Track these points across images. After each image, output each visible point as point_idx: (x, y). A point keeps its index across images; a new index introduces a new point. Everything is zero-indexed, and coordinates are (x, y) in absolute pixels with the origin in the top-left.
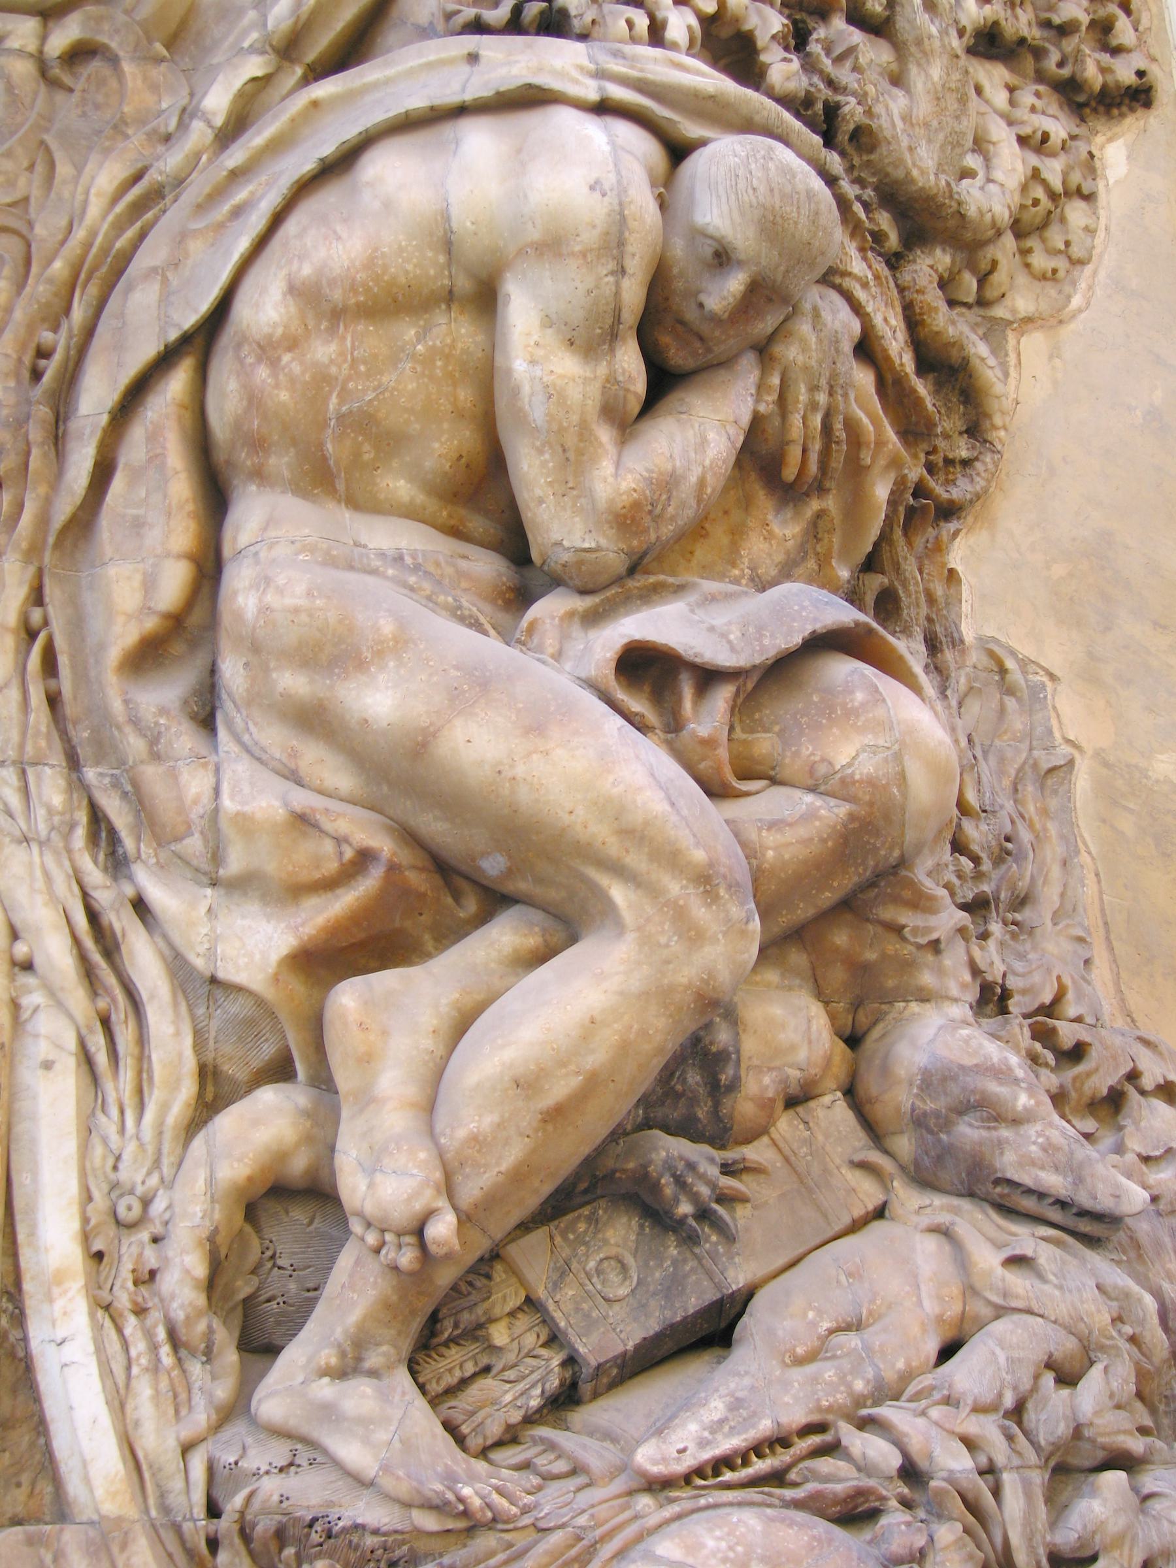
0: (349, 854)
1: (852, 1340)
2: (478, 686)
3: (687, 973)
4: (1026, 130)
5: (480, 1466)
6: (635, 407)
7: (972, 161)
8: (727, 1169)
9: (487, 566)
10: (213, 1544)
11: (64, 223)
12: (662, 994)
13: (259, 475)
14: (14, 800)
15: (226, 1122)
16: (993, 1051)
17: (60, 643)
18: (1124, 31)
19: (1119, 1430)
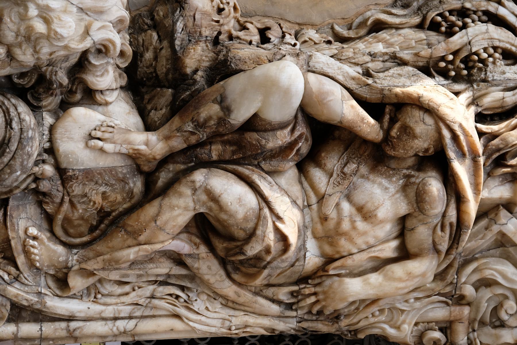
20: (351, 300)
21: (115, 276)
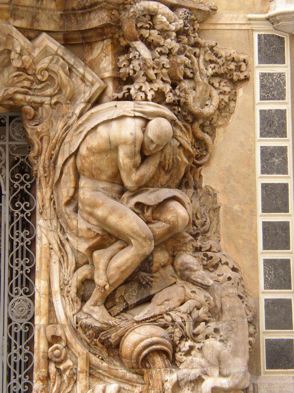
0: (95, 234)
1: (167, 302)
2: (113, 210)
3: (141, 252)
4: (221, 91)
5: (114, 318)
6: (138, 165)
7: (207, 103)
8: (152, 277)
9: (117, 188)
10: (77, 328)
11: (54, 133)
13: (84, 175)
14: (50, 225)
15: (79, 270)
17: (56, 201)
18: (244, 67)
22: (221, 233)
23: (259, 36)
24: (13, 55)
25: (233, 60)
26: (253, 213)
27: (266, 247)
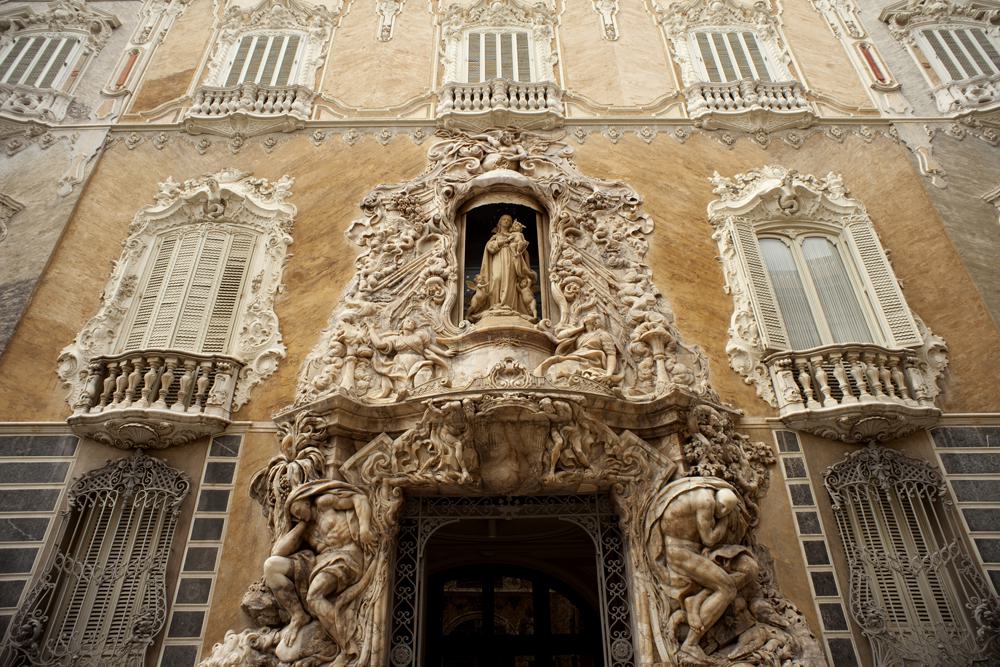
9: (697, 545)
12: (726, 600)
15: (674, 614)
16: (767, 604)
19: (789, 654)
20: (367, 530)
21: (352, 633)
22: (778, 582)
23: (777, 433)
24: (606, 446)
25: (763, 449)
26: (802, 564)
27: (818, 593)
